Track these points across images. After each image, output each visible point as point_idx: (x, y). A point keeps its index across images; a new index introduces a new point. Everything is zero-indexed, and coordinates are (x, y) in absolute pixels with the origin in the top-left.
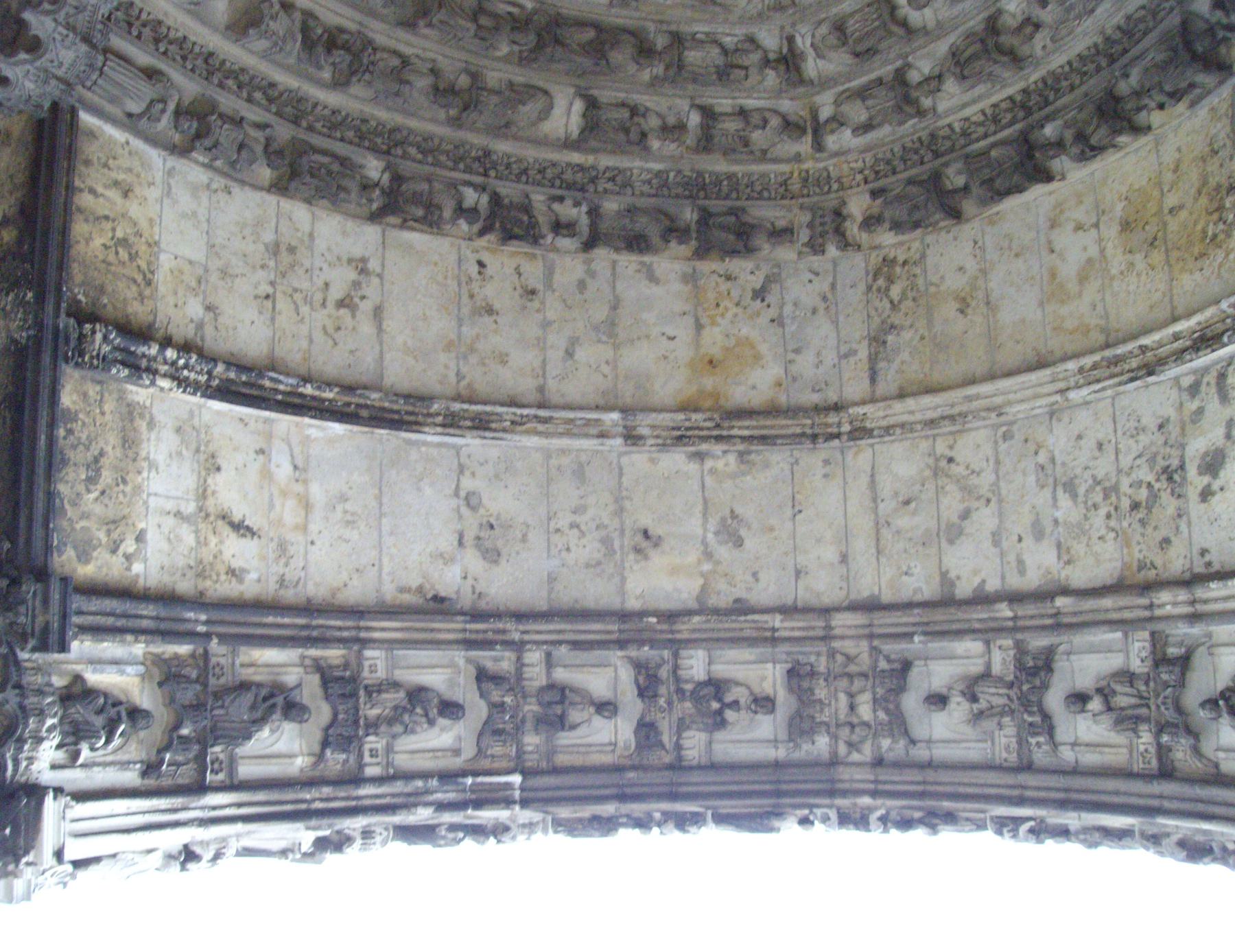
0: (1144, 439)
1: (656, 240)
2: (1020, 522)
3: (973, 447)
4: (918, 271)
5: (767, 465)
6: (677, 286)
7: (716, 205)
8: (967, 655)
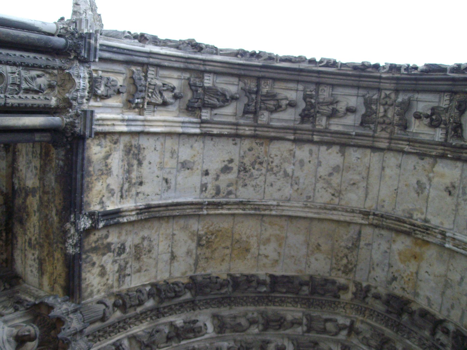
0: (254, 183)
1: (417, 313)
2: (309, 168)
3: (323, 197)
4: (334, 266)
5: (403, 211)
6: (421, 293)
7: (393, 317)
8: (336, 125)
